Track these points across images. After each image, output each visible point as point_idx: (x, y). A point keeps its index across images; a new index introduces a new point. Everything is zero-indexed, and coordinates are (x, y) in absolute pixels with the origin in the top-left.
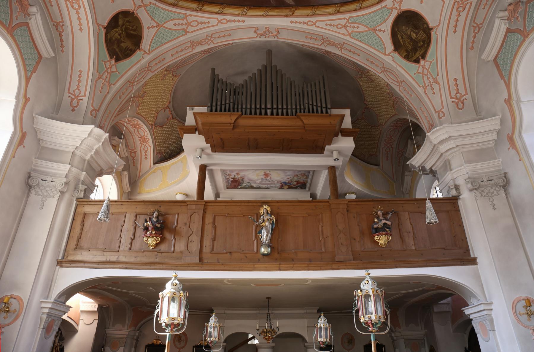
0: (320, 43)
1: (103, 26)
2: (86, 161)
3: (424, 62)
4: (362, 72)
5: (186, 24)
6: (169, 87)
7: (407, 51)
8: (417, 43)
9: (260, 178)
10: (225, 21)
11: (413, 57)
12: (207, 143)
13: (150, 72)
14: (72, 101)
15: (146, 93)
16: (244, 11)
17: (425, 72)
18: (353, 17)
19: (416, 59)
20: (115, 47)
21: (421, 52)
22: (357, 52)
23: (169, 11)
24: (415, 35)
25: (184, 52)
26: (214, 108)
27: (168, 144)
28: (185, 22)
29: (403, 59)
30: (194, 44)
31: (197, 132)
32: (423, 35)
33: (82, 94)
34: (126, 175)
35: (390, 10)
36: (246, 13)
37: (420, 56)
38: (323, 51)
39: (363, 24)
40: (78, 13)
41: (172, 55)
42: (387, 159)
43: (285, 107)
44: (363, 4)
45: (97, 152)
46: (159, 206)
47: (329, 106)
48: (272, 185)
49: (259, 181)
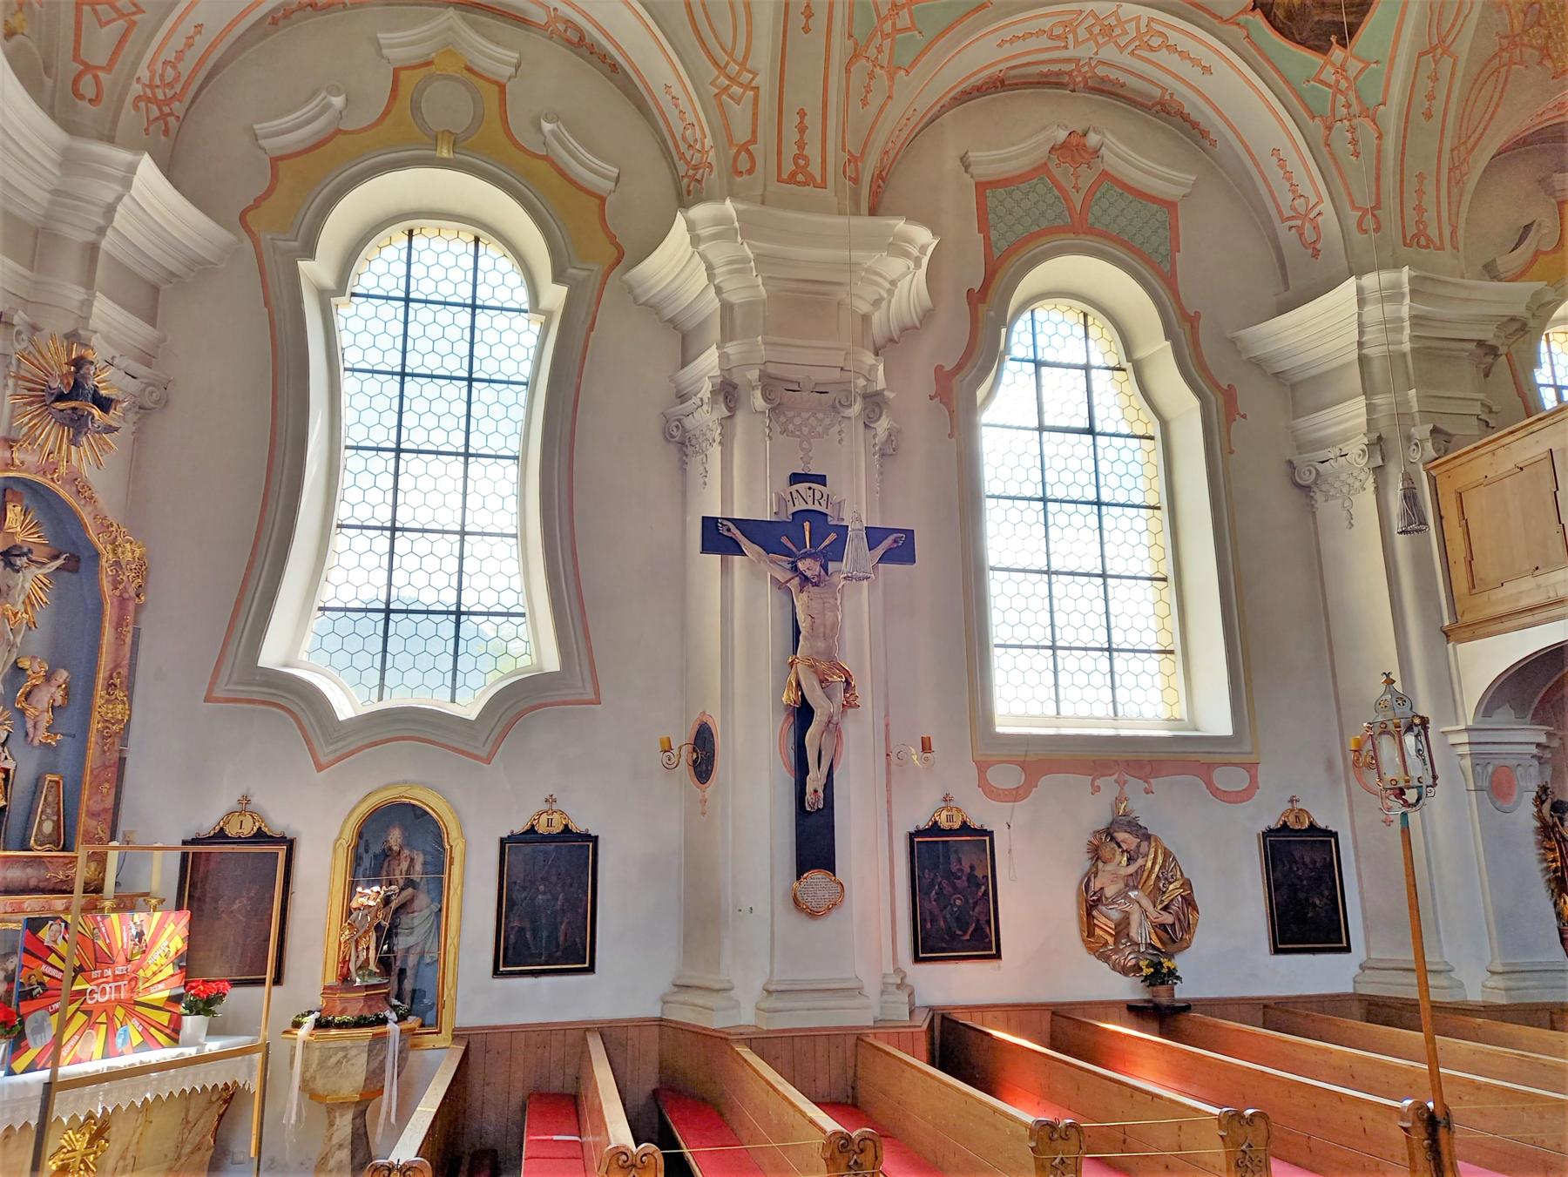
14: (1301, 235)
33: (1313, 200)
40: (1172, 49)
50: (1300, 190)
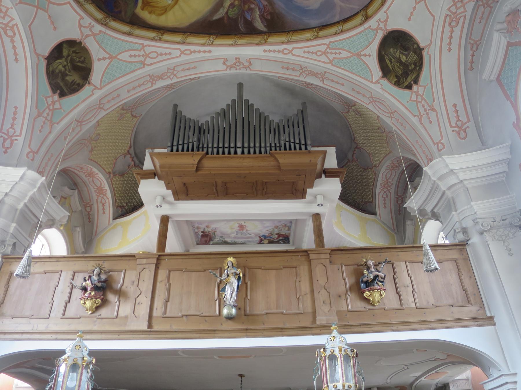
0: (298, 73)
1: (43, 56)
2: (19, 211)
3: (417, 87)
4: (348, 105)
5: (143, 56)
6: (129, 130)
7: (397, 76)
8: (408, 66)
9: (234, 230)
10: (188, 52)
11: (404, 82)
12: (168, 188)
13: (102, 110)
15: (99, 135)
16: (210, 40)
17: (419, 99)
18: (334, 42)
19: (408, 85)
20: (59, 81)
21: (412, 76)
22: (341, 81)
23: (123, 41)
24: (404, 57)
25: (143, 88)
26: (175, 148)
27: (131, 196)
28: (142, 53)
29: (394, 86)
30: (153, 78)
31: (156, 177)
32: (414, 56)
33: (18, 133)
34: (79, 232)
35: (375, 32)
36: (212, 42)
37: (412, 80)
38: (302, 83)
39: (346, 49)
40: (12, 41)
41: (128, 91)
42: (385, 207)
43: (257, 145)
44: (343, 27)
45: (32, 199)
46: (103, 261)
47: (309, 142)
48: (249, 240)
49: (233, 235)
50: (15, 127)
